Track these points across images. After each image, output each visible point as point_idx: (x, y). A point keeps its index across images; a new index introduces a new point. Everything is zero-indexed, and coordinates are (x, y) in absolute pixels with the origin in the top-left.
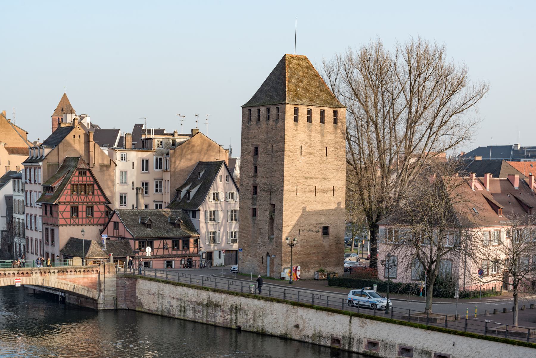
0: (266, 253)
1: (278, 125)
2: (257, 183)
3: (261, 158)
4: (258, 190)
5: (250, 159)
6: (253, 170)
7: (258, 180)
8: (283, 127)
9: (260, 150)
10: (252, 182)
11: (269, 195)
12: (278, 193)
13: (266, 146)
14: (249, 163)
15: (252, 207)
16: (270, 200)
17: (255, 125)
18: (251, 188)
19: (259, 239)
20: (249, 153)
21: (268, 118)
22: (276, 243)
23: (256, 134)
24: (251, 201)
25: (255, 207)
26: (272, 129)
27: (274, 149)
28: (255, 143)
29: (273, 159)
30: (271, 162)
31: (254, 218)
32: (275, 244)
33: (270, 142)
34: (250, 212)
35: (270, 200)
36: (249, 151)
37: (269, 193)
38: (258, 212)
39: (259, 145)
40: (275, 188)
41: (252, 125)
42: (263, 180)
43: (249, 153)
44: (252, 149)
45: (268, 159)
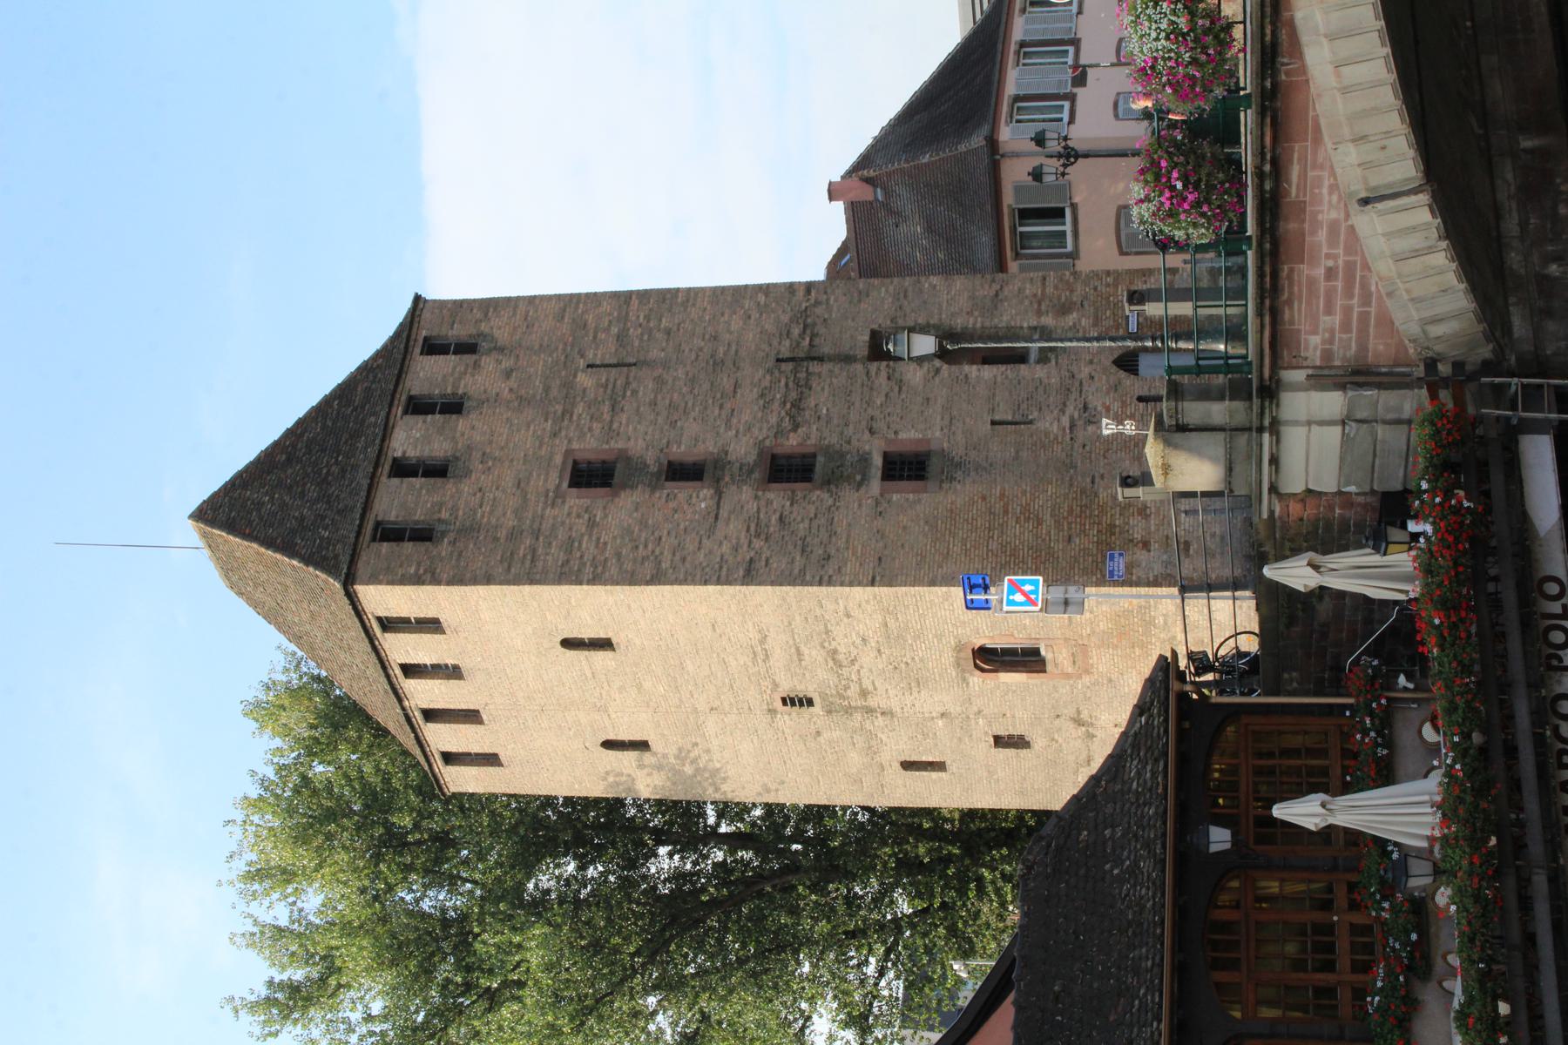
0: (1122, 374)
1: (502, 335)
2: (751, 458)
3: (640, 438)
4: (792, 443)
5: (620, 511)
6: (682, 491)
7: (742, 449)
8: (522, 307)
9: (590, 446)
10: (746, 493)
11: (827, 366)
12: (819, 310)
13: (579, 409)
14: (643, 524)
15: (875, 485)
16: (848, 359)
17: (466, 487)
18: (777, 497)
19: (1049, 424)
20: (592, 524)
21: (453, 407)
22: (1064, 309)
23: (509, 481)
24: (848, 495)
25: (878, 461)
26: (508, 374)
27: (606, 351)
28: (554, 477)
29: (655, 354)
30: (666, 365)
31: (934, 465)
32: (1071, 319)
33: (568, 385)
34: (902, 494)
35: (848, 359)
36: (581, 526)
37: (815, 367)
38: (909, 436)
39: (568, 452)
40: (796, 331)
41: (455, 509)
42: (746, 417)
43: (592, 524)
44: (577, 500)
45: (646, 387)
